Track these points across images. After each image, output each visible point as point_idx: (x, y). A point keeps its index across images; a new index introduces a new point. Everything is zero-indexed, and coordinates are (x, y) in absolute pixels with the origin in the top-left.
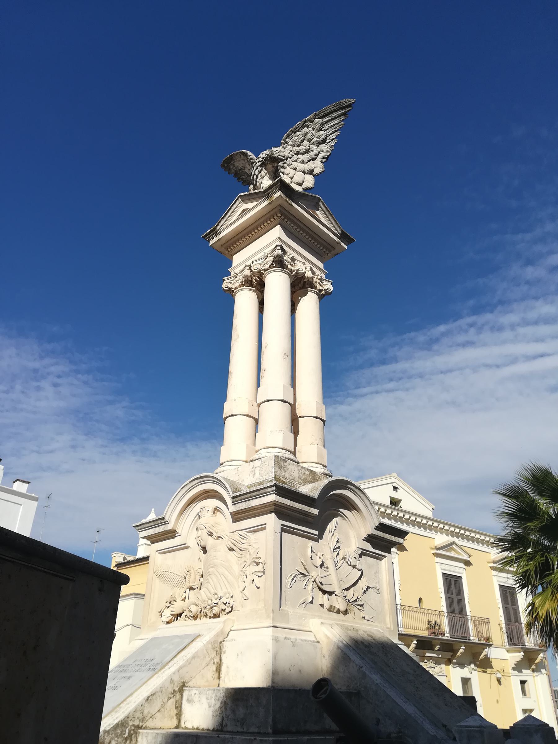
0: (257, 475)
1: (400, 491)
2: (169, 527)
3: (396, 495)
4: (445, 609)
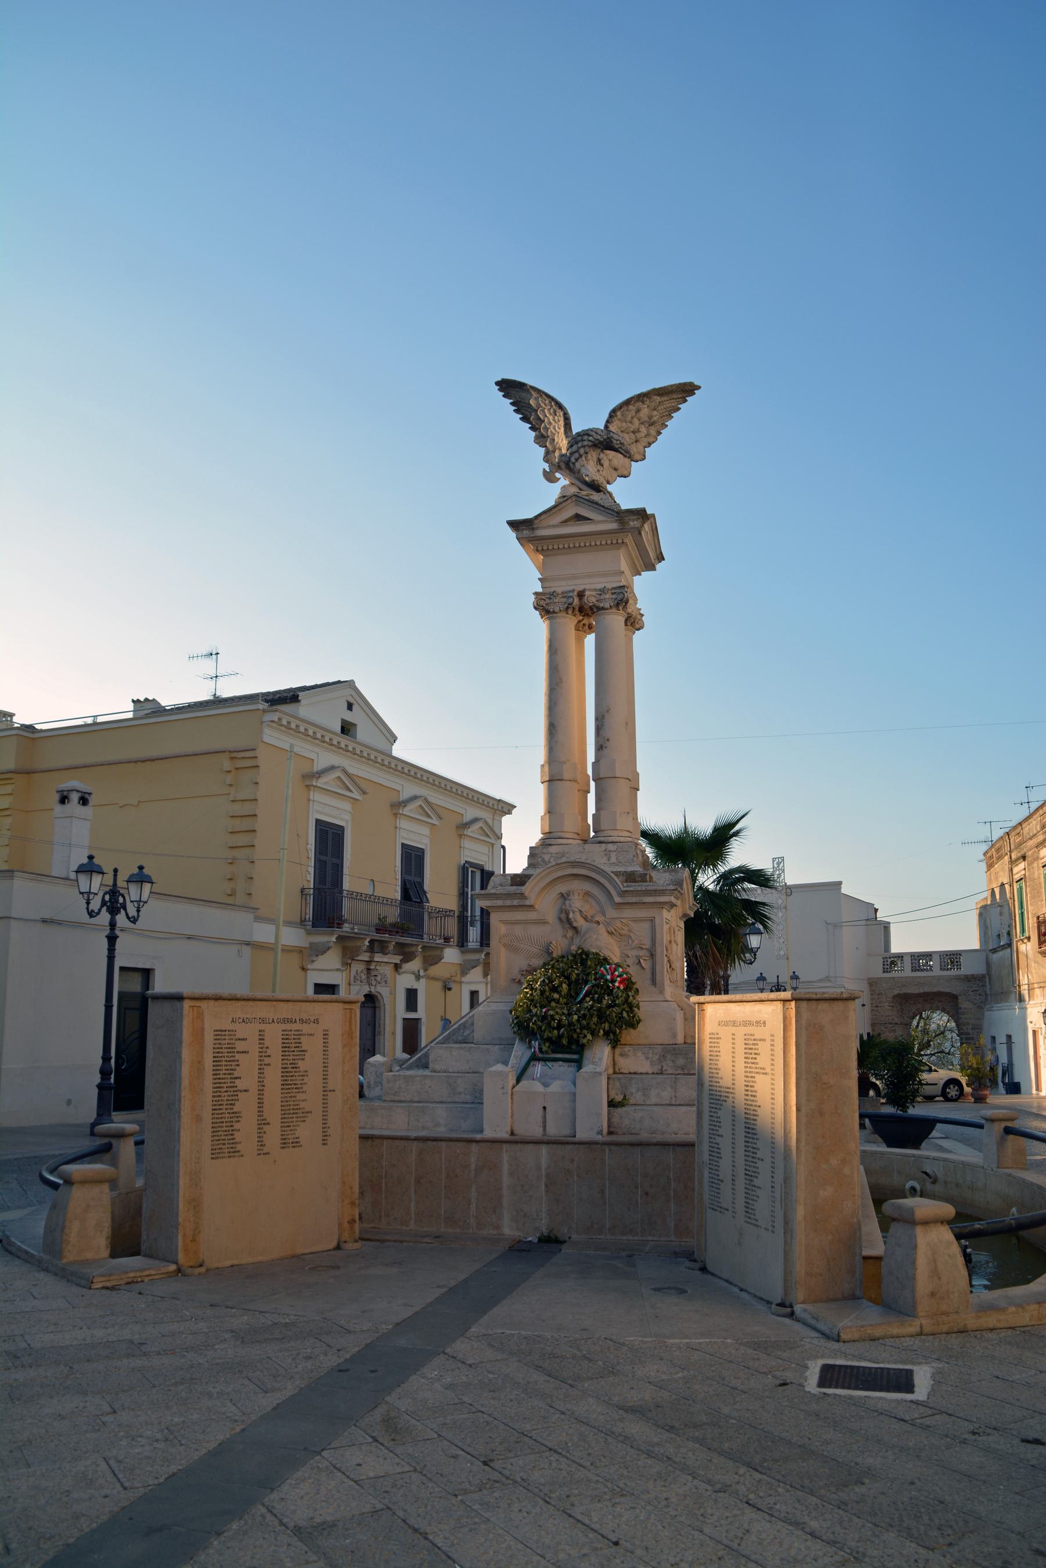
0: (613, 859)
1: (355, 707)
2: (528, 903)
3: (349, 717)
4: (398, 896)
